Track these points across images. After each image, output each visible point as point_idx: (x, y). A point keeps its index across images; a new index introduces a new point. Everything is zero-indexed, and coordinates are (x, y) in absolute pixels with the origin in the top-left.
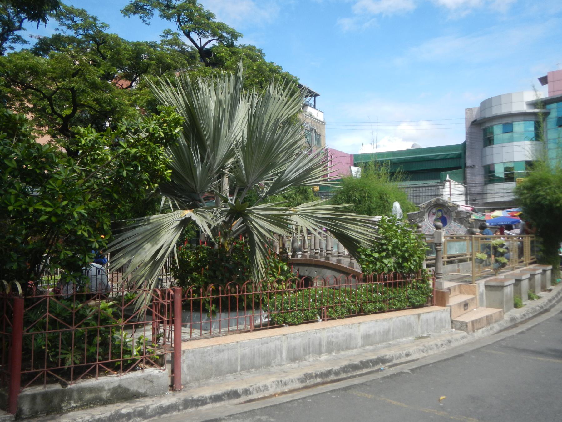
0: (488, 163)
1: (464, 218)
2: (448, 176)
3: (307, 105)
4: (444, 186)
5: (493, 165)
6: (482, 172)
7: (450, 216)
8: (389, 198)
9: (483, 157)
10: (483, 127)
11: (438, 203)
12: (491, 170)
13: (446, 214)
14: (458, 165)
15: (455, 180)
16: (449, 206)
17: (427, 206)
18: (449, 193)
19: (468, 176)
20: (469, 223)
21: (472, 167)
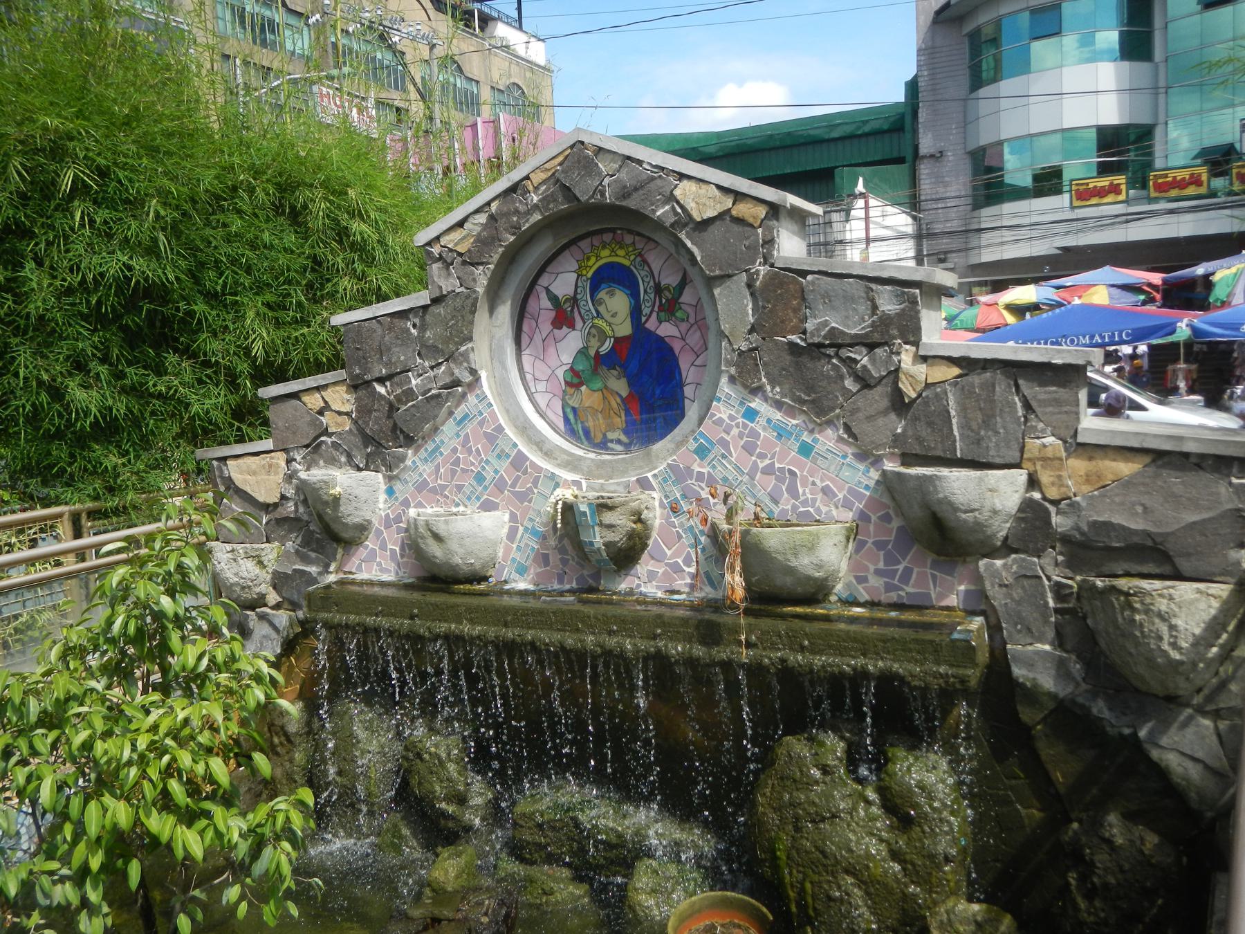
1: (838, 342)
2: (861, 180)
3: (494, 19)
4: (848, 215)
5: (1000, 143)
6: (966, 166)
7: (701, 325)
8: (357, 213)
10: (969, 27)
11: (584, 192)
13: (669, 308)
14: (895, 155)
15: (880, 195)
17: (485, 242)
18: (863, 235)
19: (926, 187)
20: (899, 404)
21: (938, 157)
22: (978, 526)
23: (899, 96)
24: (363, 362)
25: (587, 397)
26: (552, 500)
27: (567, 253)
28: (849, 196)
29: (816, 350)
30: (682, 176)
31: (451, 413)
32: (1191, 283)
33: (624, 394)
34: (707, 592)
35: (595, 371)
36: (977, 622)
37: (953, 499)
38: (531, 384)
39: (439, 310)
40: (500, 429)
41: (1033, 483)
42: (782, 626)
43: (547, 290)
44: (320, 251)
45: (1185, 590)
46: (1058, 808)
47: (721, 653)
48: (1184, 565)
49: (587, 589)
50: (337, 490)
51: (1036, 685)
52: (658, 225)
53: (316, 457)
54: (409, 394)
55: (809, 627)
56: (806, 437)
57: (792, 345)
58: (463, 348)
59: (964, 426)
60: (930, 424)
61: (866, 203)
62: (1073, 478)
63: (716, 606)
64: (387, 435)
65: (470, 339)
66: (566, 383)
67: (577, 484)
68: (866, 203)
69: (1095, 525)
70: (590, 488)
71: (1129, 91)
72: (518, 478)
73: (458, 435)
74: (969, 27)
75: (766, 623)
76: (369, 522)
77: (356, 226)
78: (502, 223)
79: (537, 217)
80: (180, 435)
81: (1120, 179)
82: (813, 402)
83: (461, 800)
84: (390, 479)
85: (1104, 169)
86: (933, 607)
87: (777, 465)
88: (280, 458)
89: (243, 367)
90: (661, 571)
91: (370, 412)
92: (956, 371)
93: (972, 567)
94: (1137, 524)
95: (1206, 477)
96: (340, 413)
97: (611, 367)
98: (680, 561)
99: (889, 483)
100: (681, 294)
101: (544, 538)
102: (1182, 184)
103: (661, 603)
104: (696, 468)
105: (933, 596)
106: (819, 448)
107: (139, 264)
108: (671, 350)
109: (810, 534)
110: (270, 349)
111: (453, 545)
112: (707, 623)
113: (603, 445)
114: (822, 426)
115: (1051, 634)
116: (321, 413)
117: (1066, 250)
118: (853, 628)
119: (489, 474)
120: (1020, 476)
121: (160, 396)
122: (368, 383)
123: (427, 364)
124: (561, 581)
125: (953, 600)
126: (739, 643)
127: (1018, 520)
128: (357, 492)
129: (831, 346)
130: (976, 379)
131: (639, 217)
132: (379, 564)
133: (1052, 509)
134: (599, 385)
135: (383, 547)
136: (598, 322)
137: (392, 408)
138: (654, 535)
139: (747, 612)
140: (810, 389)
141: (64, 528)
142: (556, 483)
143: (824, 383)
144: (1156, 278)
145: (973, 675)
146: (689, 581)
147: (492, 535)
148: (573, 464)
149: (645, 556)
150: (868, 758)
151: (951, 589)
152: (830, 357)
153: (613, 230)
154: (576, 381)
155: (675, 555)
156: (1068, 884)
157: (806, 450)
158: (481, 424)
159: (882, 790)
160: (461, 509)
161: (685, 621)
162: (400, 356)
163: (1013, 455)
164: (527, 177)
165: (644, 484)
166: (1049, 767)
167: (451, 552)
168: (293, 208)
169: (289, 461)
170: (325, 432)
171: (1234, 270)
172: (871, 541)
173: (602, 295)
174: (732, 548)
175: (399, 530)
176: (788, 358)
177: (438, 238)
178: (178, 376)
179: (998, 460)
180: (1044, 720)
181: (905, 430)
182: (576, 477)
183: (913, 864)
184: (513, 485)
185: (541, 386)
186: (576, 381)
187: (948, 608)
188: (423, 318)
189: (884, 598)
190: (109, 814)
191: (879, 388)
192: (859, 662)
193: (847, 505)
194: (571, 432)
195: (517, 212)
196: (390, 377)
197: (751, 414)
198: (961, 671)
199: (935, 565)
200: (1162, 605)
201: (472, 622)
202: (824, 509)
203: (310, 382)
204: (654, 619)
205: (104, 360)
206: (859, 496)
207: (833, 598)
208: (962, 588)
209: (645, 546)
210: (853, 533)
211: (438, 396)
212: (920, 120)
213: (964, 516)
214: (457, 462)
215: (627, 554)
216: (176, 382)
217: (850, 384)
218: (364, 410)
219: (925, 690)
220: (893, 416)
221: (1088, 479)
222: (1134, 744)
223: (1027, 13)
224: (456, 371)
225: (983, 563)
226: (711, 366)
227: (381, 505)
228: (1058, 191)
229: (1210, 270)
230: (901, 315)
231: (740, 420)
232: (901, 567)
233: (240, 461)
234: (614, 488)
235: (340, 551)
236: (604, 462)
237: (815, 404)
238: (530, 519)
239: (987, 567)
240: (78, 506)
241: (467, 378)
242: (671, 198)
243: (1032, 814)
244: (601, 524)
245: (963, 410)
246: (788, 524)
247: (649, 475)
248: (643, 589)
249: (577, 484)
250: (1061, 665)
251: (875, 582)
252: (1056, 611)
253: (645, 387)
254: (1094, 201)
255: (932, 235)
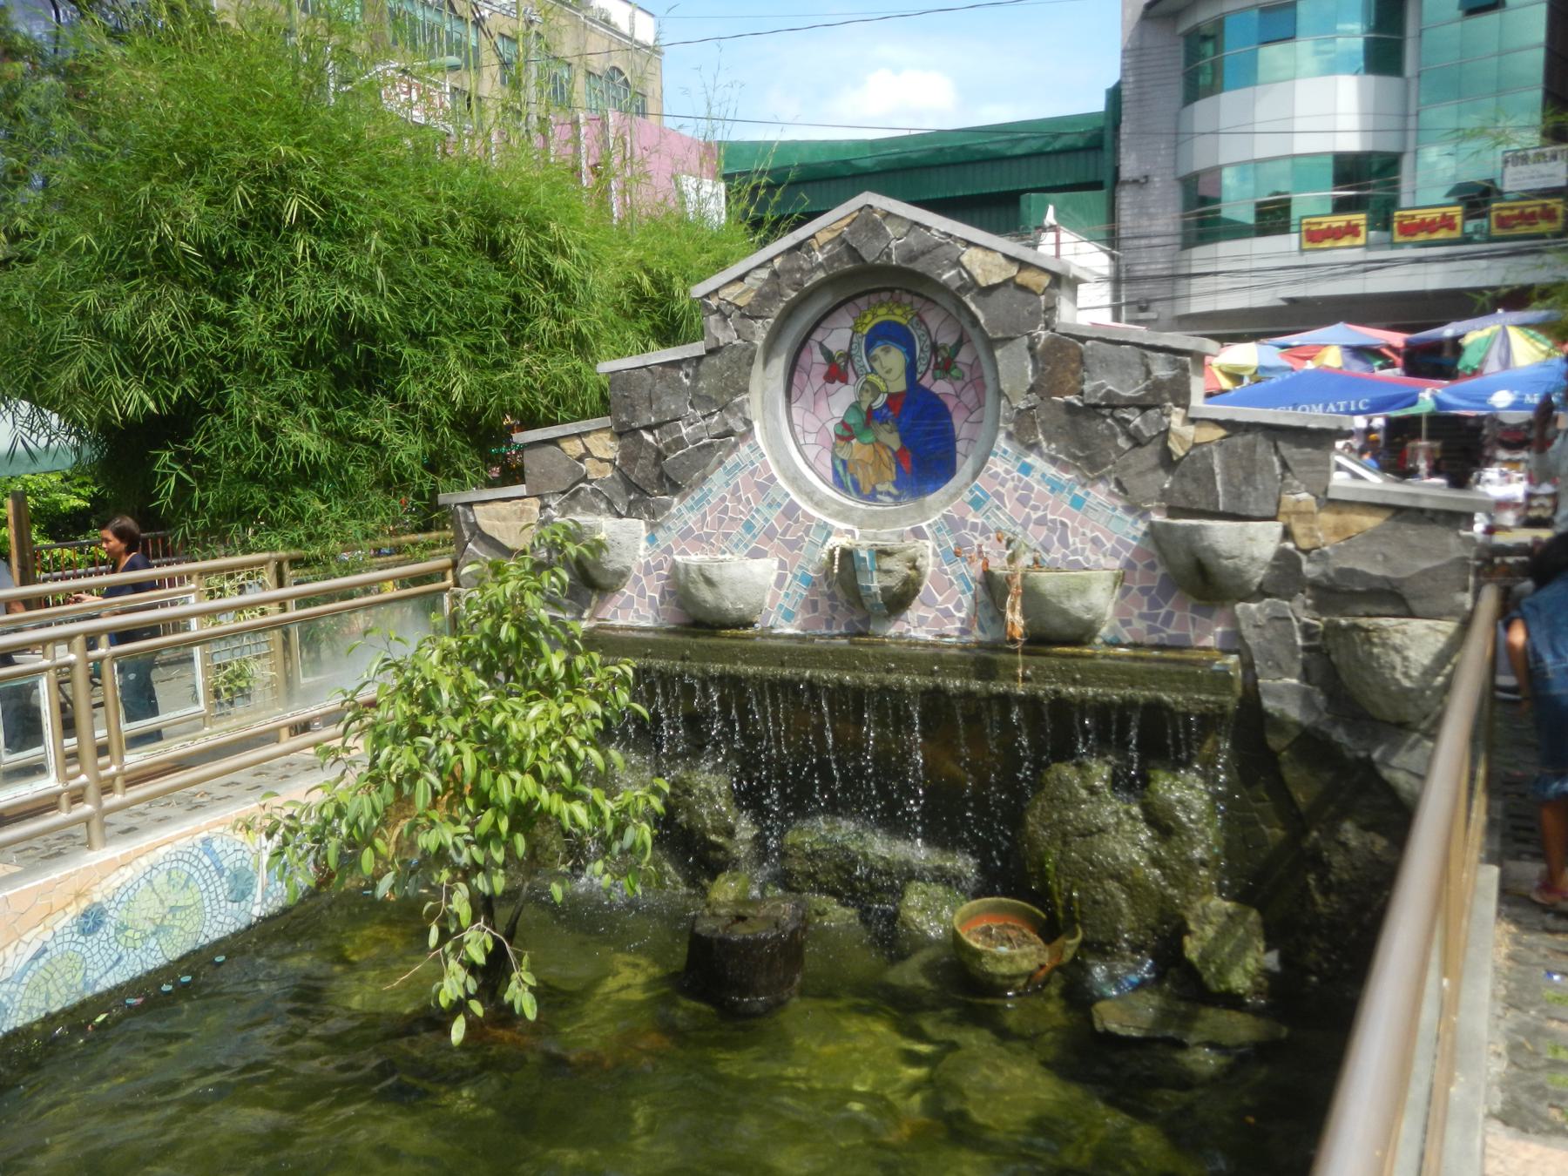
0: (1200, 163)
1: (1113, 403)
2: (1051, 209)
5: (1217, 170)
6: (1176, 195)
7: (981, 384)
8: (558, 248)
9: (1179, 137)
10: (1184, 26)
11: (870, 254)
12: (1204, 190)
13: (945, 367)
14: (1091, 178)
15: (1074, 228)
16: (971, 285)
17: (765, 297)
19: (1126, 217)
20: (1168, 461)
21: (1141, 182)
22: (1238, 572)
23: (1098, 104)
24: (632, 409)
25: (858, 450)
26: (828, 546)
27: (843, 310)
28: (1037, 228)
29: (1092, 410)
30: (969, 244)
31: (721, 463)
32: (1437, 347)
33: (896, 447)
34: (977, 635)
35: (867, 425)
36: (1233, 659)
37: (1216, 546)
38: (800, 437)
39: (716, 361)
40: (772, 479)
41: (1287, 534)
42: (1055, 662)
43: (821, 344)
44: (524, 292)
45: (1417, 626)
46: (1297, 822)
47: (999, 687)
48: (1416, 606)
49: (854, 633)
50: (602, 536)
51: (1283, 715)
52: (943, 288)
53: (573, 503)
54: (679, 443)
55: (1080, 663)
56: (1078, 491)
57: (1070, 407)
58: (738, 400)
59: (1228, 482)
60: (1196, 480)
61: (1058, 238)
62: (1323, 530)
63: (994, 647)
64: (651, 482)
65: (746, 390)
66: (838, 436)
67: (851, 532)
68: (1058, 238)
69: (1342, 572)
70: (863, 536)
71: (1374, 116)
72: (789, 526)
73: (727, 484)
74: (1184, 26)
75: (1038, 660)
76: (629, 569)
77: (559, 264)
78: (784, 280)
79: (821, 275)
80: (377, 484)
81: (1359, 218)
82: (1087, 458)
83: (730, 832)
84: (652, 527)
85: (1341, 206)
86: (1191, 647)
87: (1050, 517)
88: (534, 505)
89: (445, 414)
90: (931, 616)
91: (635, 459)
92: (1221, 432)
93: (1228, 610)
94: (1377, 571)
95: (1438, 530)
96: (601, 460)
97: (884, 420)
98: (951, 607)
99: (1154, 533)
100: (957, 353)
101: (814, 584)
102: (1430, 226)
103: (933, 645)
104: (971, 519)
105: (1192, 636)
106: (1090, 501)
107: (359, 300)
108: (945, 407)
109: (1082, 578)
110: (468, 395)
111: (725, 590)
112: (984, 661)
113: (872, 497)
114: (1094, 481)
115: (1298, 669)
116: (581, 459)
117: (1293, 301)
118: (1121, 663)
119: (759, 522)
120: (1276, 528)
121: (364, 440)
122: (635, 431)
123: (698, 413)
124: (829, 627)
125: (1210, 641)
126: (1015, 678)
127: (1273, 567)
128: (620, 538)
129: (1106, 407)
130: (1239, 440)
131: (923, 278)
132: (637, 611)
133: (1303, 557)
134: (870, 438)
135: (642, 594)
136: (872, 378)
137: (660, 456)
138: (926, 582)
139: (1025, 653)
140: (1084, 446)
141: (268, 576)
142: (829, 532)
143: (1098, 441)
144: (1398, 339)
145: (1231, 702)
146: (958, 625)
147: (764, 584)
148: (844, 514)
149: (916, 602)
150: (1131, 784)
151: (1208, 631)
152: (1105, 417)
153: (892, 290)
154: (847, 434)
155: (946, 601)
156: (1307, 884)
157: (1077, 503)
158: (753, 473)
159: (1145, 807)
160: (728, 556)
161: (961, 660)
162: (670, 405)
163: (1270, 509)
164: (813, 236)
165: (918, 533)
166: (1293, 790)
167: (722, 597)
168: (493, 243)
169: (543, 507)
170: (585, 479)
171: (1487, 332)
172: (1135, 587)
173: (877, 351)
174: (1013, 590)
175: (659, 577)
176: (1064, 418)
177: (716, 291)
178: (380, 420)
179: (1256, 514)
180: (1289, 747)
181: (1172, 485)
182: (849, 527)
183: (1172, 869)
184: (784, 533)
185: (811, 439)
186: (847, 434)
187: (1206, 649)
188: (696, 368)
189: (1148, 639)
190: (518, 785)
191: (1150, 448)
192: (1129, 692)
193: (1115, 554)
194: (839, 484)
195: (800, 269)
196: (659, 425)
197: (1026, 469)
198: (1221, 698)
199: (1195, 609)
200: (1397, 639)
201: (746, 662)
202: (1093, 558)
203: (572, 428)
204: (930, 658)
205: (314, 401)
206: (1126, 546)
207: (1098, 641)
208: (1219, 629)
209: (917, 591)
210: (1121, 579)
211: (710, 445)
212: (1123, 137)
213: (1225, 562)
214: (725, 511)
215: (899, 601)
216: (380, 426)
217: (1122, 442)
218: (628, 457)
219: (1187, 715)
220: (1161, 473)
221: (1336, 531)
222: (1369, 766)
223: (1256, 13)
224: (731, 421)
225: (1239, 607)
226: (988, 420)
227: (641, 552)
228: (1284, 229)
229: (1460, 331)
230: (1173, 380)
231: (1016, 474)
232: (1163, 611)
233: (488, 507)
234: (887, 537)
235: (595, 598)
236: (875, 512)
237: (1088, 459)
238: (801, 567)
239: (1244, 610)
240: (282, 554)
241: (741, 428)
242: (958, 263)
243: (1275, 833)
244: (879, 570)
245: (1227, 468)
246: (1058, 570)
247: (924, 525)
248: (913, 633)
249: (851, 532)
250: (1307, 698)
251: (1139, 625)
252: (1305, 649)
253: (918, 442)
254: (1327, 244)
255: (1132, 280)
